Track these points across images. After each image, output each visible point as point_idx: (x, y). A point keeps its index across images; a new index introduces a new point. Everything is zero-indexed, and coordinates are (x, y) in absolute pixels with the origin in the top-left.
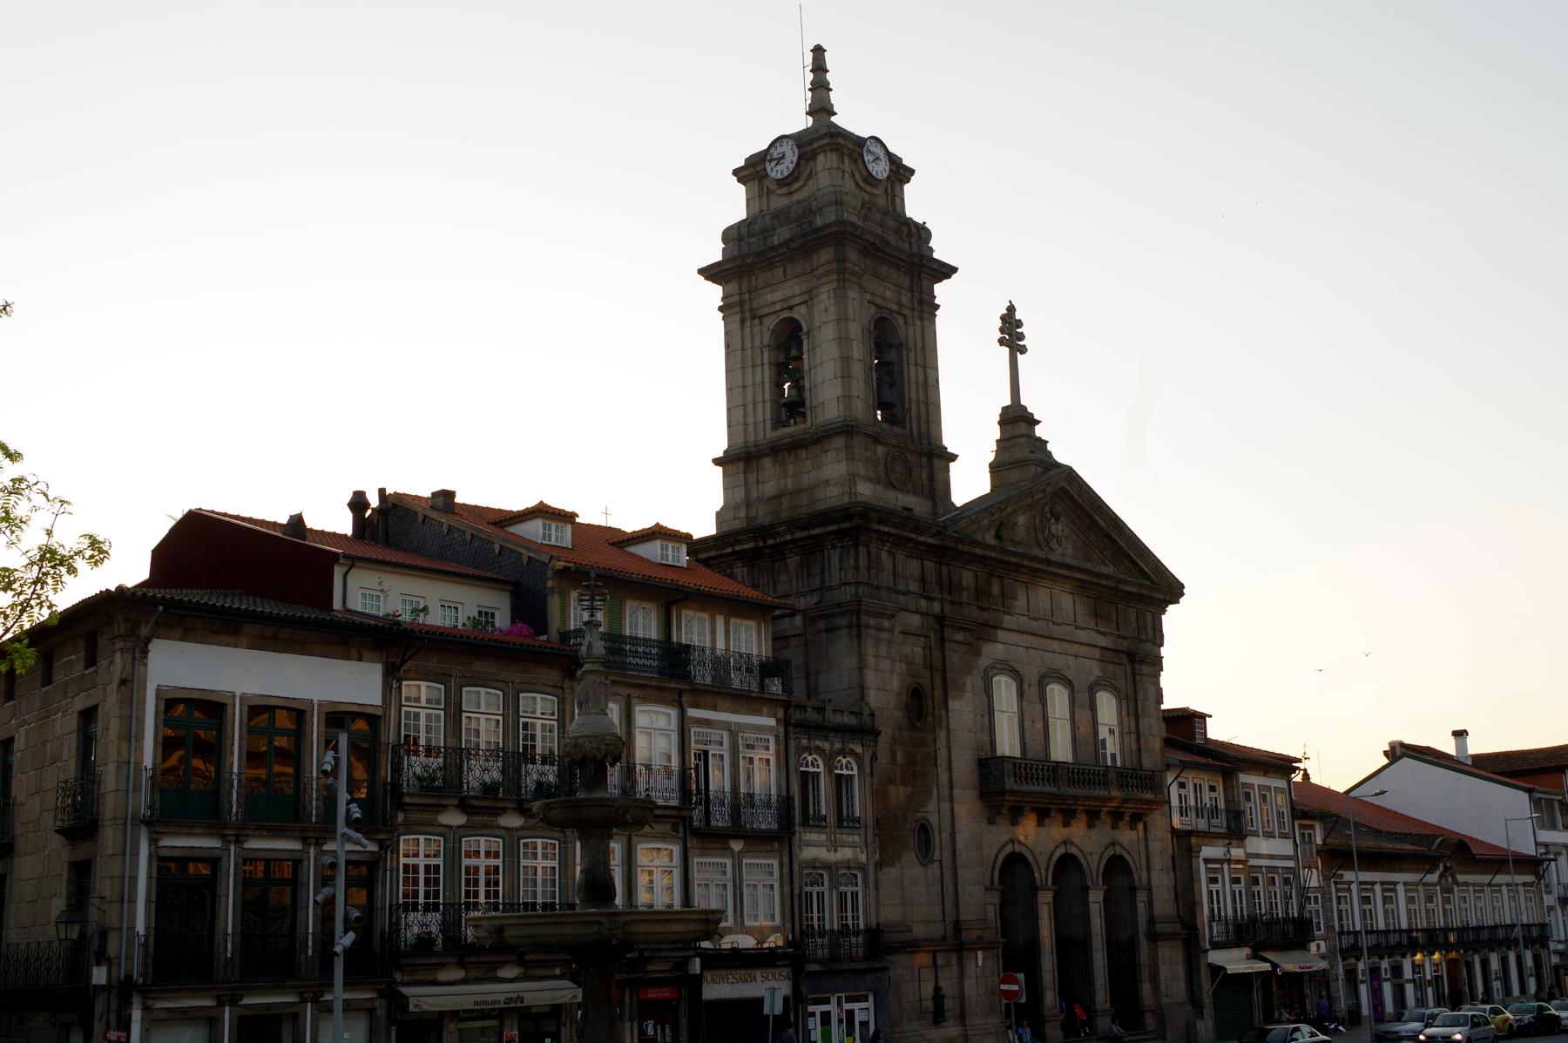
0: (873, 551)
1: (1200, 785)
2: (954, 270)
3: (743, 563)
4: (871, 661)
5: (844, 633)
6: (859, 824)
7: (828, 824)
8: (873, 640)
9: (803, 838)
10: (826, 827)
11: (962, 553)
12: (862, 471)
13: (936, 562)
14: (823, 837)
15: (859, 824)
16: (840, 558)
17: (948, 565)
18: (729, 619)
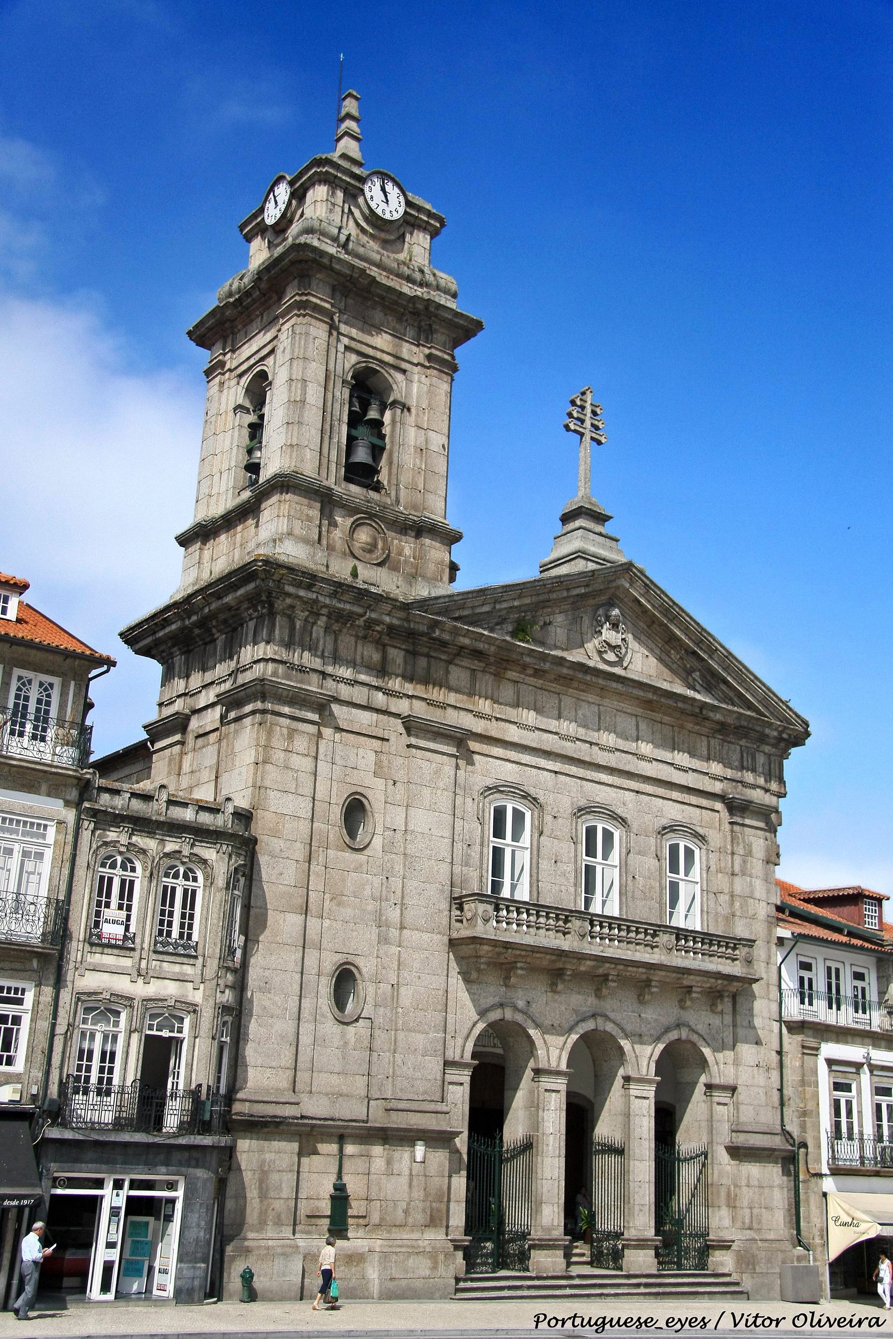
0: (298, 624)
1: (837, 970)
2: (478, 326)
3: (179, 649)
4: (278, 756)
5: (247, 721)
6: (133, 943)
7: (138, 947)
8: (285, 731)
9: (89, 959)
10: (133, 949)
11: (444, 644)
12: (297, 531)
13: (407, 651)
14: (126, 963)
15: (133, 943)
16: (255, 627)
17: (428, 656)
18: (11, 669)
